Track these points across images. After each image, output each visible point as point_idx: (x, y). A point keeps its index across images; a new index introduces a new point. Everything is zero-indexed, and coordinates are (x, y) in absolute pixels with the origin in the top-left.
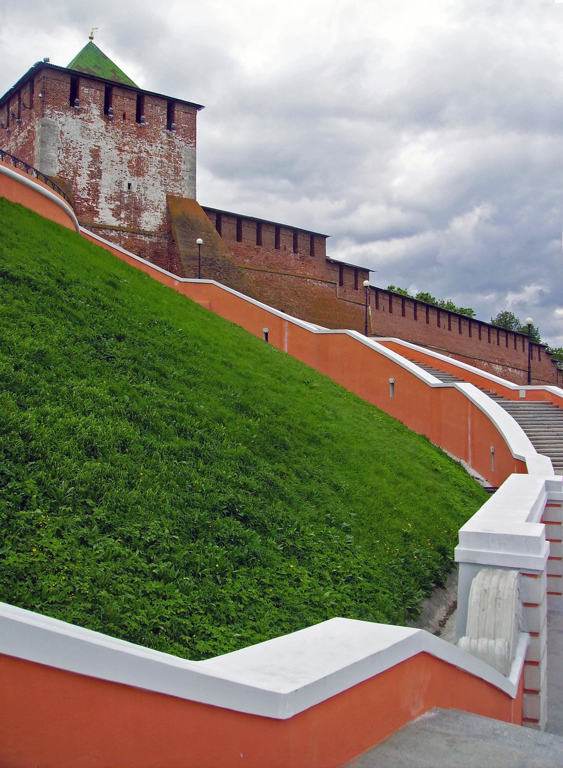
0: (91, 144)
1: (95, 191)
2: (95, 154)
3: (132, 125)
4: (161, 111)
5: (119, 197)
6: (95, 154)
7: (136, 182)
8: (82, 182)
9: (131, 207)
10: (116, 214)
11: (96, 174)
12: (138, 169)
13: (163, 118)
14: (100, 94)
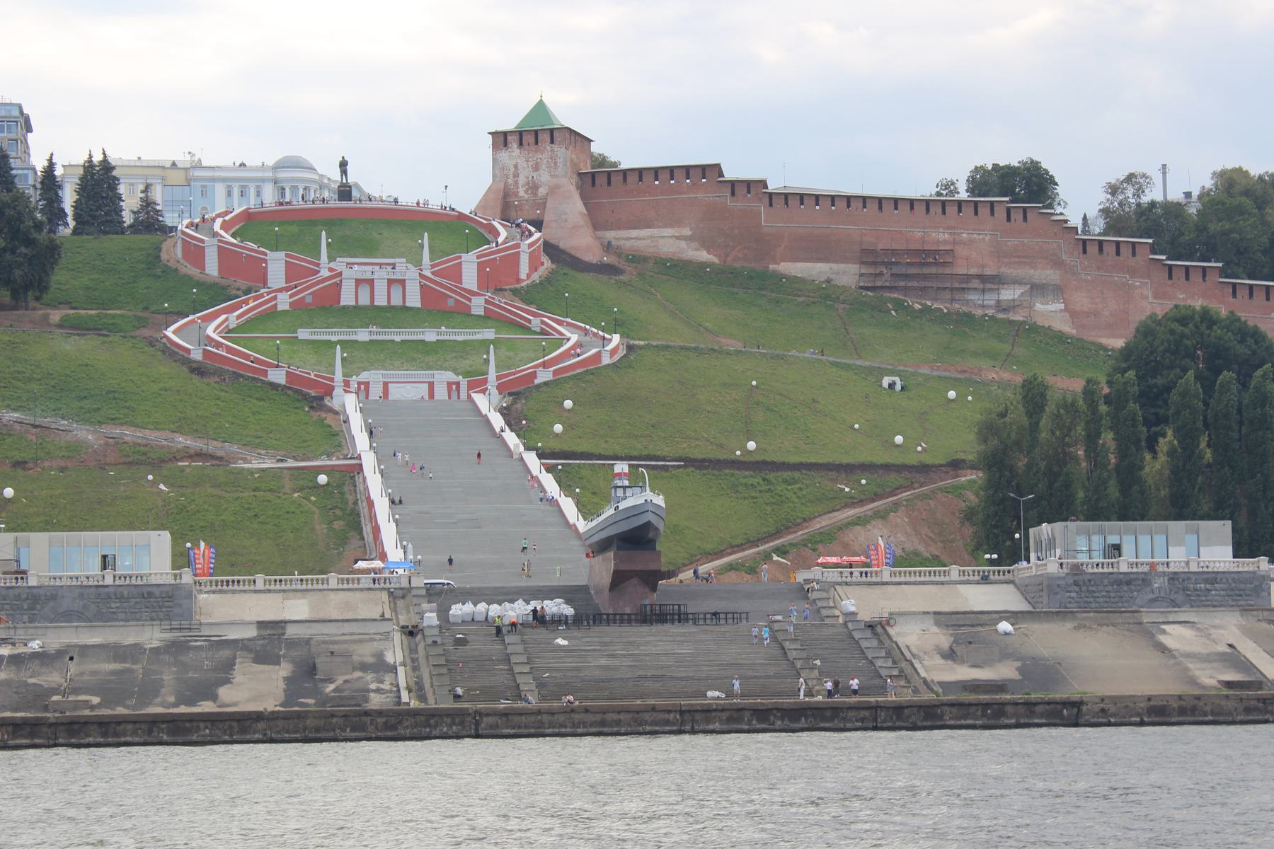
0: (514, 162)
1: (516, 182)
2: (516, 166)
3: (533, 147)
4: (547, 137)
5: (528, 183)
6: (516, 166)
7: (535, 175)
8: (510, 181)
9: (533, 187)
10: (526, 192)
11: (516, 176)
12: (536, 168)
13: (548, 139)
14: (516, 137)
